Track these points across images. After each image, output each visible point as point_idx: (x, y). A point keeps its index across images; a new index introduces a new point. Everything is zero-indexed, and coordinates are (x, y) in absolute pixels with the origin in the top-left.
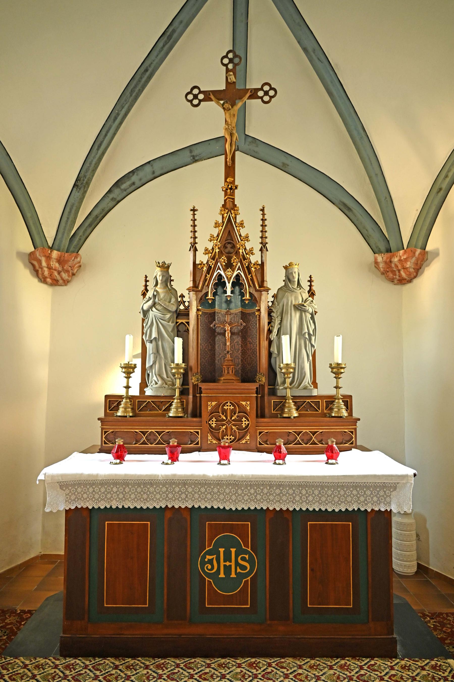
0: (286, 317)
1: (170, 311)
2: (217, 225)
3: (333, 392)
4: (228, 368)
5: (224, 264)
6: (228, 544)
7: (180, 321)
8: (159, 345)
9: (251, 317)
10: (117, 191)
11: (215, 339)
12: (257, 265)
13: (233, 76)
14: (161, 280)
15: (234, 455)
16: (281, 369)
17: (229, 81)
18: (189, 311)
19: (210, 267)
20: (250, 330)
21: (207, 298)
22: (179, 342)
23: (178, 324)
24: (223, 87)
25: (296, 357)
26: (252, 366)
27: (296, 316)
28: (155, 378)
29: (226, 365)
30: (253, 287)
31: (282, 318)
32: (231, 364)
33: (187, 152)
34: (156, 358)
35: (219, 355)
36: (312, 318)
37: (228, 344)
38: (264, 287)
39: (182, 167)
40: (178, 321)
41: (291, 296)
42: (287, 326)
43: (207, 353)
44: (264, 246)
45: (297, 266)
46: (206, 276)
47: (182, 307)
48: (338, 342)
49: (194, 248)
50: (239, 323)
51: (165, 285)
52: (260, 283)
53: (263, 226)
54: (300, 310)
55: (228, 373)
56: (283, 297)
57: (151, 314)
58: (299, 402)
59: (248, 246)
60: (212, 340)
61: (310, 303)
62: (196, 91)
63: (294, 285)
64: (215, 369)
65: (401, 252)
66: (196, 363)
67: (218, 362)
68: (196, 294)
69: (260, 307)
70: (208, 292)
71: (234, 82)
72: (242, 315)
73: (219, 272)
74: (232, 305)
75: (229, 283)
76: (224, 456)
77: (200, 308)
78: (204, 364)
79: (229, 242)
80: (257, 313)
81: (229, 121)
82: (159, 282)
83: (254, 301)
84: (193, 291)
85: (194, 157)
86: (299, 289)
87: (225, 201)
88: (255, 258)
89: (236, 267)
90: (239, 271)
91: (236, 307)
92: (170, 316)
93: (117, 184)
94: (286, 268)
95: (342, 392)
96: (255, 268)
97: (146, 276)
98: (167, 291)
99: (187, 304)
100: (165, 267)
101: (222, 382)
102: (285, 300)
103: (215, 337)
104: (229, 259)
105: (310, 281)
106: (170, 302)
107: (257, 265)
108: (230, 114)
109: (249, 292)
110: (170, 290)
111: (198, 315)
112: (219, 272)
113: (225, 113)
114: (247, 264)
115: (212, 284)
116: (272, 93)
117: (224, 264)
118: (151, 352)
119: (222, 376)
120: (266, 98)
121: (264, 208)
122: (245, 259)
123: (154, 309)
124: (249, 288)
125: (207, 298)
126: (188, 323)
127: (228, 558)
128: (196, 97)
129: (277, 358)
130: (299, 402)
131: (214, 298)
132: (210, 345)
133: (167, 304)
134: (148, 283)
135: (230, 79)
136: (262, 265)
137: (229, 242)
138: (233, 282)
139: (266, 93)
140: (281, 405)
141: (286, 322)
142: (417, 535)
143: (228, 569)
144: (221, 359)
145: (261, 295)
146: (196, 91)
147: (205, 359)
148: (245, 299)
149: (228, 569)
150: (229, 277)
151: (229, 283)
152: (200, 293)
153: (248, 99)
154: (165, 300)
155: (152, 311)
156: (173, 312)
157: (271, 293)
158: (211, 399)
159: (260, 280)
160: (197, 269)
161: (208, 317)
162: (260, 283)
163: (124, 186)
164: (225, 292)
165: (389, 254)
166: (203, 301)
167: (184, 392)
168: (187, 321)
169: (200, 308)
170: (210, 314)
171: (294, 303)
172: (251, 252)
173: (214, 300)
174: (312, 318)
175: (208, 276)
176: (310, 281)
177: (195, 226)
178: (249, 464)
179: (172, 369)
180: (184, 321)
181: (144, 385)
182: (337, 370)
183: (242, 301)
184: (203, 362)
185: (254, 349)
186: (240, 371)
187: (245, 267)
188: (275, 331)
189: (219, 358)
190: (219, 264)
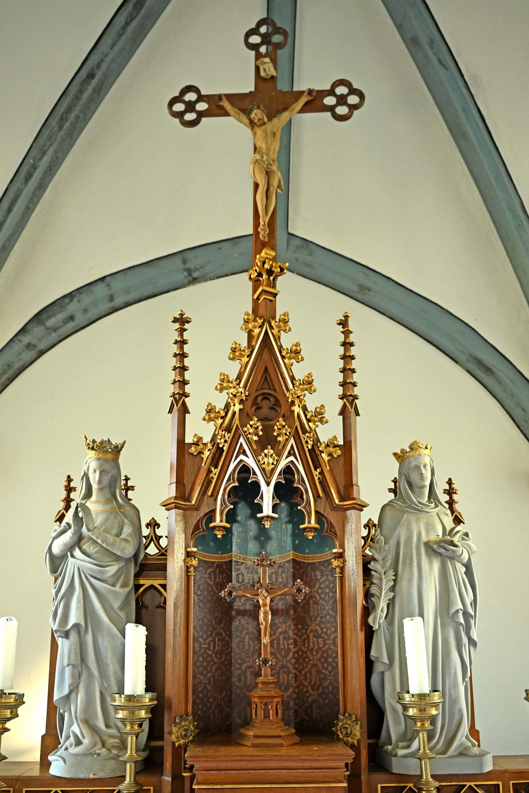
0: (407, 571)
1: (118, 558)
2: (235, 352)
4: (266, 704)
5: (256, 438)
7: (146, 582)
8: (86, 642)
9: (318, 573)
11: (231, 625)
12: (335, 446)
13: (271, 65)
14: (100, 482)
16: (405, 708)
17: (262, 74)
18: (166, 559)
20: (316, 603)
21: (212, 525)
23: (142, 589)
24: (249, 87)
26: (323, 692)
29: (259, 697)
30: (324, 499)
31: (396, 575)
32: (273, 693)
33: (177, 262)
34: (76, 679)
35: (241, 664)
36: (469, 572)
37: (265, 640)
38: (354, 499)
39: (168, 291)
40: (141, 582)
41: (418, 520)
42: (410, 594)
43: (212, 660)
44: (352, 403)
45: (427, 452)
46: (209, 471)
47: (152, 550)
49: (180, 405)
50: (290, 588)
51: (109, 496)
52: (342, 490)
54: (440, 554)
55: (267, 716)
56: (397, 524)
60: (223, 628)
61: (463, 539)
62: (191, 97)
63: (421, 495)
64: (230, 700)
66: (183, 691)
67: (240, 681)
68: (184, 516)
69: (342, 546)
70: (214, 511)
71: (273, 77)
72: (294, 568)
73: (241, 461)
74: (272, 546)
75: (268, 484)
77: (195, 550)
78: (205, 688)
80: (335, 563)
81: (264, 146)
82: (95, 486)
83: (329, 533)
84: (176, 507)
85: (189, 271)
86: (433, 505)
87: (256, 301)
89: (285, 446)
90: (292, 458)
91: (281, 549)
92: (119, 570)
96: (330, 455)
97: (69, 477)
98: (113, 508)
99: (163, 542)
101: (249, 743)
102: (402, 532)
103: (231, 619)
106: (118, 535)
107: (335, 446)
108: (266, 132)
109: (317, 512)
110: (120, 506)
111: (188, 568)
112: (241, 461)
113: (255, 134)
114: (311, 443)
115: (225, 490)
117: (256, 438)
118: (66, 664)
119: (247, 722)
121: (346, 317)
122: (304, 431)
123: (77, 552)
124: (315, 501)
125: (212, 525)
126: (164, 586)
129: (387, 675)
131: (228, 525)
132: (219, 640)
133: (111, 539)
134: (72, 495)
135: (265, 70)
138: (277, 484)
139: (340, 101)
141: (408, 586)
144: (245, 673)
145: (344, 521)
146: (191, 97)
147: (205, 676)
148: (305, 529)
150: (269, 468)
151: (268, 484)
152: (195, 513)
153: (302, 110)
154: (106, 531)
155: (72, 556)
156: (128, 560)
157: (366, 515)
159: (342, 483)
160: (186, 456)
161: (214, 572)
162: (342, 490)
164: (260, 509)
166: (201, 532)
168: (162, 582)
169: (195, 550)
170: (219, 565)
171: (424, 538)
173: (228, 531)
174: (469, 572)
175: (216, 471)
177: (182, 356)
179: (117, 708)
180: (156, 583)
181: (50, 742)
183: (298, 534)
184: (200, 682)
185: (326, 651)
186: (292, 704)
187: (306, 450)
189: (240, 672)
190: (242, 440)
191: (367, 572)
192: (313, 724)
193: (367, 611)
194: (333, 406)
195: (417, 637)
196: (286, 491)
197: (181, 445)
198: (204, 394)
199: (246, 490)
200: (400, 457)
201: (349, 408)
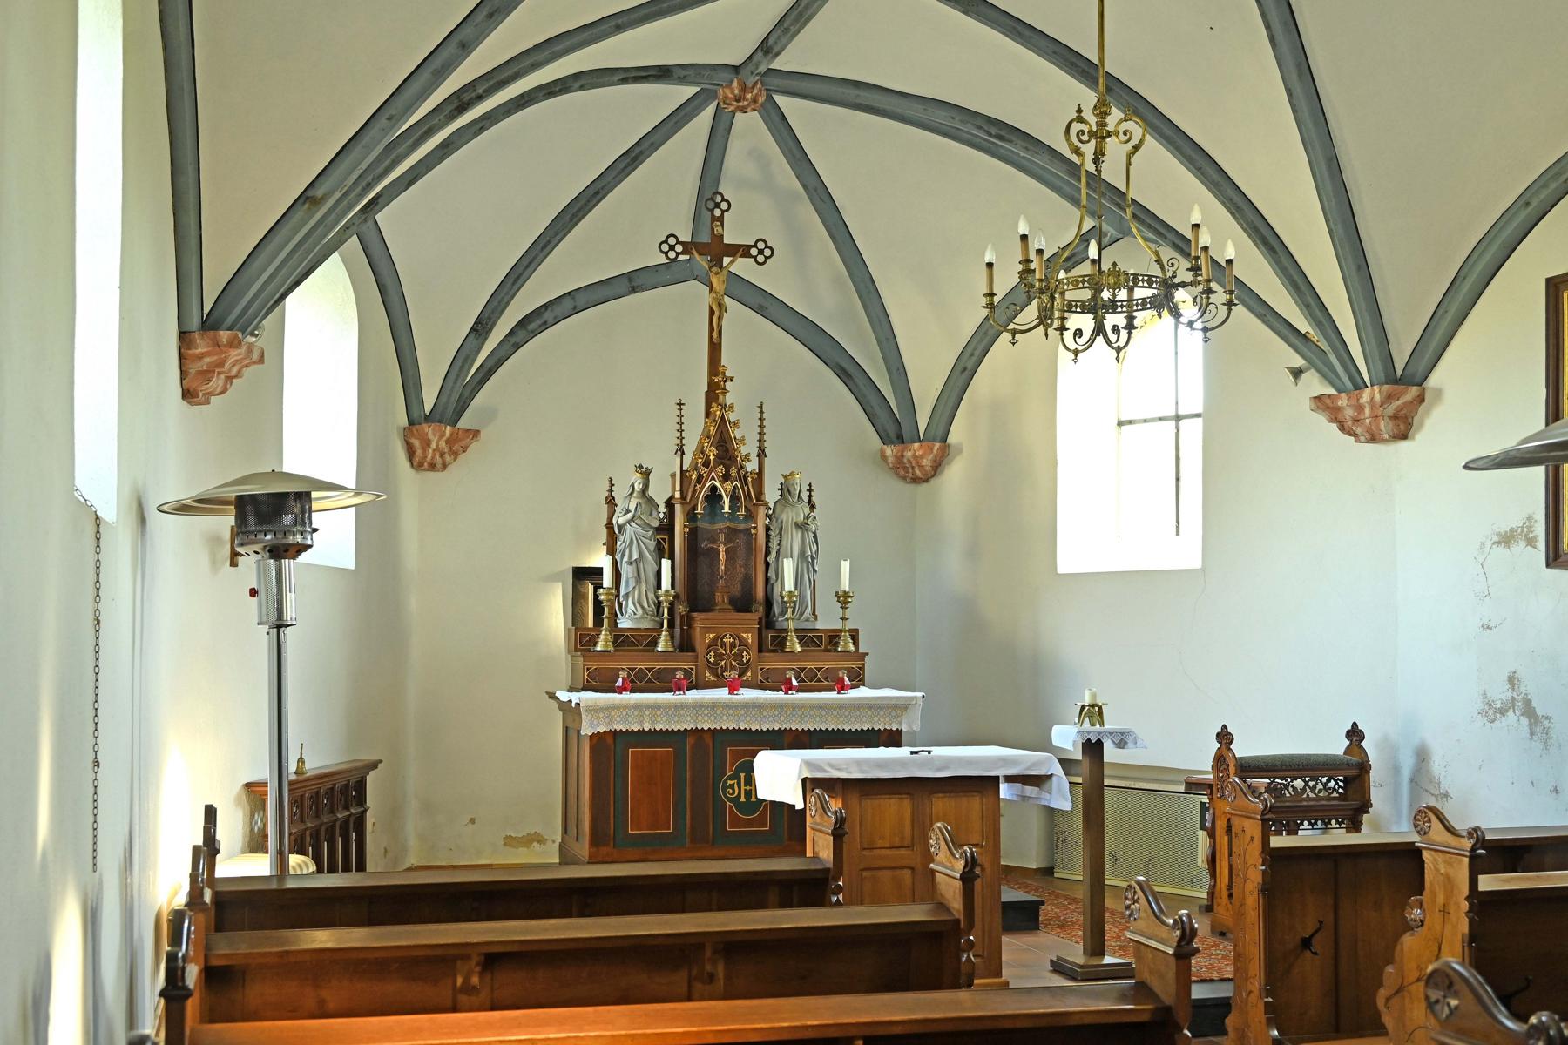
3: (838, 625)
19: (700, 476)
22: (666, 564)
25: (798, 582)
27: (797, 536)
28: (631, 605)
36: (815, 537)
48: (845, 566)
53: (761, 426)
57: (628, 529)
58: (803, 635)
59: (744, 450)
65: (916, 445)
88: (752, 466)
94: (785, 477)
95: (849, 625)
100: (646, 474)
104: (728, 469)
105: (810, 490)
116: (767, 252)
120: (761, 259)
130: (803, 635)
136: (760, 473)
137: (723, 447)
158: (709, 630)
165: (900, 447)
166: (691, 516)
167: (671, 625)
174: (815, 537)
176: (810, 490)
182: (844, 599)
188: (774, 552)
191: (767, 536)
192: (742, 604)
193: (768, 553)
194: (754, 452)
195: (789, 567)
196: (734, 498)
198: (690, 449)
199: (714, 497)
200: (785, 477)
201: (762, 454)
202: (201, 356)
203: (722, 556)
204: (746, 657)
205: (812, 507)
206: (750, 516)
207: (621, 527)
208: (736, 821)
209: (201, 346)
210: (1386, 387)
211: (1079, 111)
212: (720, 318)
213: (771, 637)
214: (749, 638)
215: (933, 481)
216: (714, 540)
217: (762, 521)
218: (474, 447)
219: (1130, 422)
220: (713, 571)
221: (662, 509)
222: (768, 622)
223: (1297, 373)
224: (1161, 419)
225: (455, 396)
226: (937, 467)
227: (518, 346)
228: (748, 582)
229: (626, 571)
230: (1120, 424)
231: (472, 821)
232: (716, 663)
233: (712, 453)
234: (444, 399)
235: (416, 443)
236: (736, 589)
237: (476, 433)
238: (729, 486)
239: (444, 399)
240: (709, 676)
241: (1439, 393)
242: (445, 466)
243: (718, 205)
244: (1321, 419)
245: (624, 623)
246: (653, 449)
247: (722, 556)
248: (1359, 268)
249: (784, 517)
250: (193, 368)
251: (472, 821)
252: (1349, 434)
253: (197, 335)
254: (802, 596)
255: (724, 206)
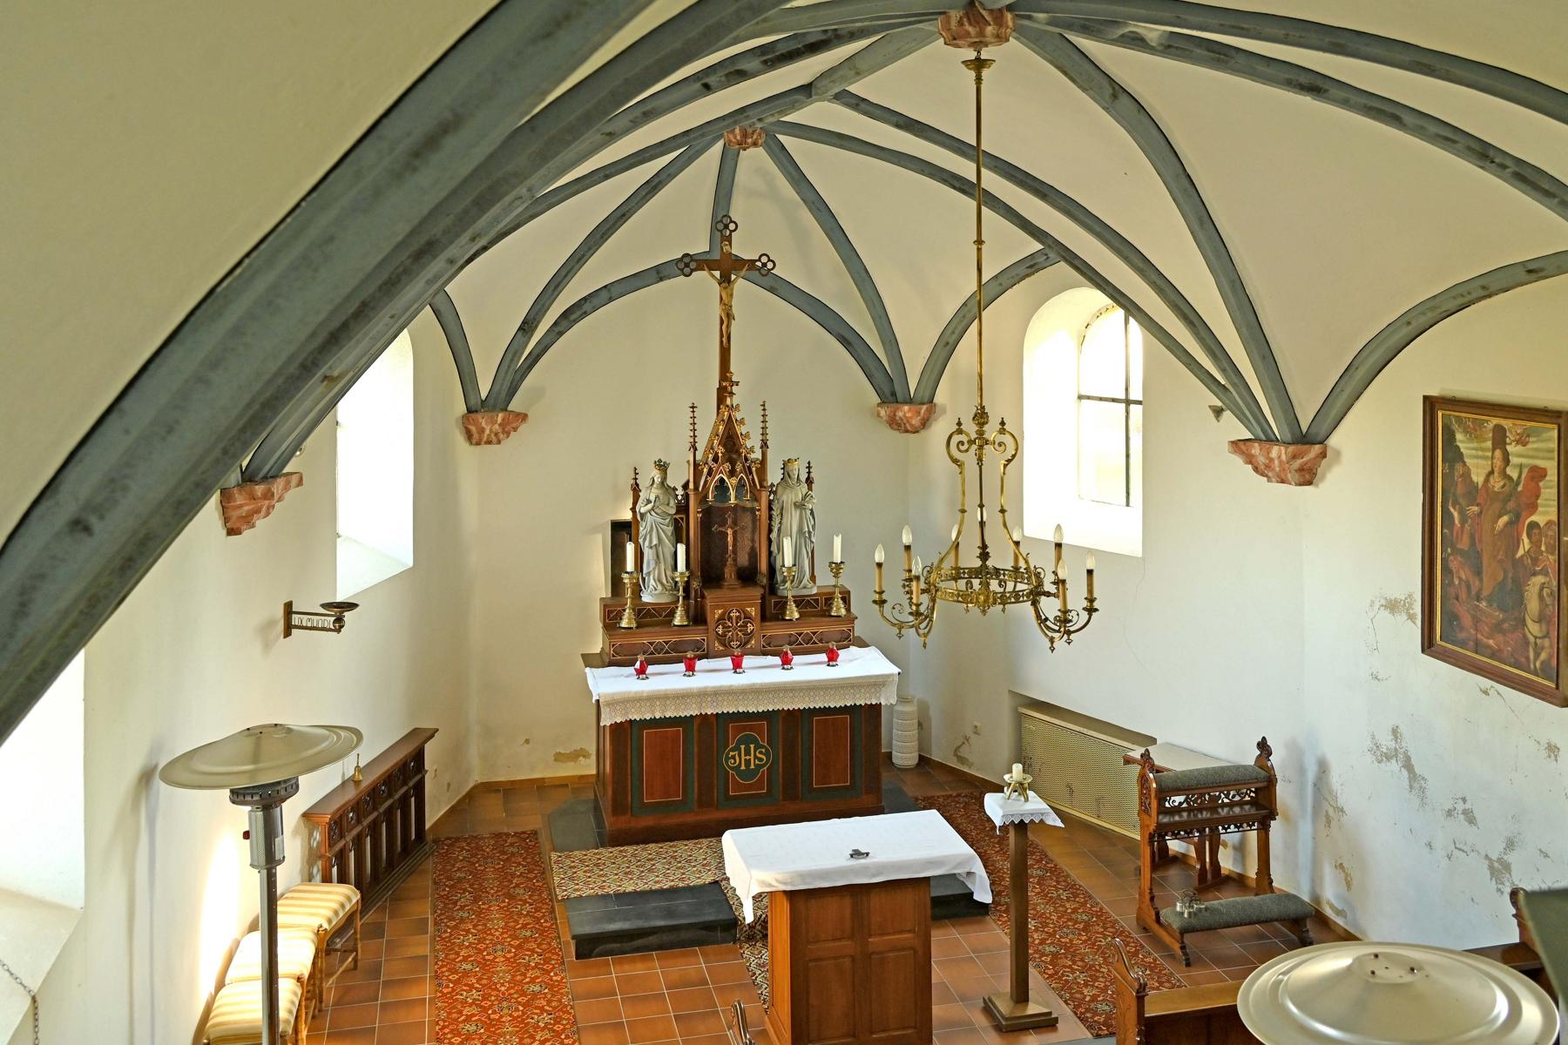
6: (747, 741)
10: (565, 323)
15: (748, 661)
22: (681, 548)
27: (796, 515)
36: (812, 513)
48: (838, 541)
58: (800, 602)
59: (749, 444)
65: (906, 408)
76: (737, 665)
79: (730, 441)
93: (565, 315)
104: (733, 464)
127: (748, 753)
128: (687, 265)
130: (800, 602)
137: (730, 441)
140: (782, 604)
142: (920, 724)
143: (748, 762)
149: (748, 762)
163: (573, 317)
167: (687, 597)
172: (752, 450)
174: (812, 513)
178: (761, 672)
182: (836, 568)
192: (747, 576)
193: (770, 531)
194: (759, 444)
195: (788, 546)
197: (696, 465)
198: (701, 446)
199: (722, 487)
201: (764, 445)
202: (241, 506)
203: (730, 539)
204: (750, 628)
205: (810, 489)
206: (756, 499)
207: (642, 515)
208: (738, 786)
209: (239, 499)
210: (1291, 448)
211: (959, 424)
212: (728, 326)
213: (772, 610)
214: (753, 611)
215: (923, 433)
216: (723, 523)
217: (764, 497)
218: (523, 428)
219: (1089, 398)
220: (722, 556)
221: (680, 492)
222: (772, 588)
223: (1218, 412)
224: (1114, 400)
225: (509, 378)
226: (925, 423)
227: (561, 334)
228: (753, 555)
229: (648, 554)
230: (1080, 397)
231: (527, 741)
232: (724, 635)
233: (720, 451)
234: (497, 388)
235: (473, 428)
236: (743, 560)
237: (523, 417)
238: (734, 481)
239: (497, 388)
240: (718, 647)
241: (1338, 454)
242: (499, 442)
243: (726, 227)
244: (1238, 460)
245: (647, 598)
246: (672, 441)
247: (730, 539)
248: (1264, 358)
249: (785, 498)
250: (235, 514)
251: (527, 741)
252: (1263, 474)
253: (235, 491)
254: (801, 570)
255: (732, 226)
